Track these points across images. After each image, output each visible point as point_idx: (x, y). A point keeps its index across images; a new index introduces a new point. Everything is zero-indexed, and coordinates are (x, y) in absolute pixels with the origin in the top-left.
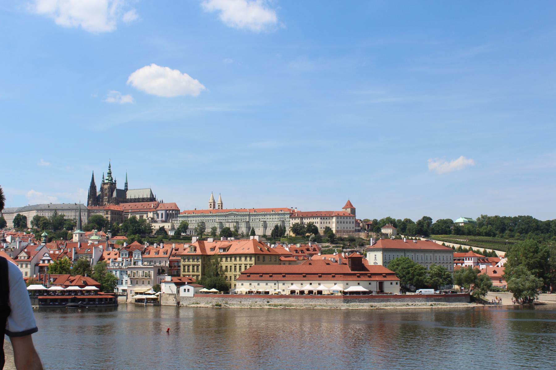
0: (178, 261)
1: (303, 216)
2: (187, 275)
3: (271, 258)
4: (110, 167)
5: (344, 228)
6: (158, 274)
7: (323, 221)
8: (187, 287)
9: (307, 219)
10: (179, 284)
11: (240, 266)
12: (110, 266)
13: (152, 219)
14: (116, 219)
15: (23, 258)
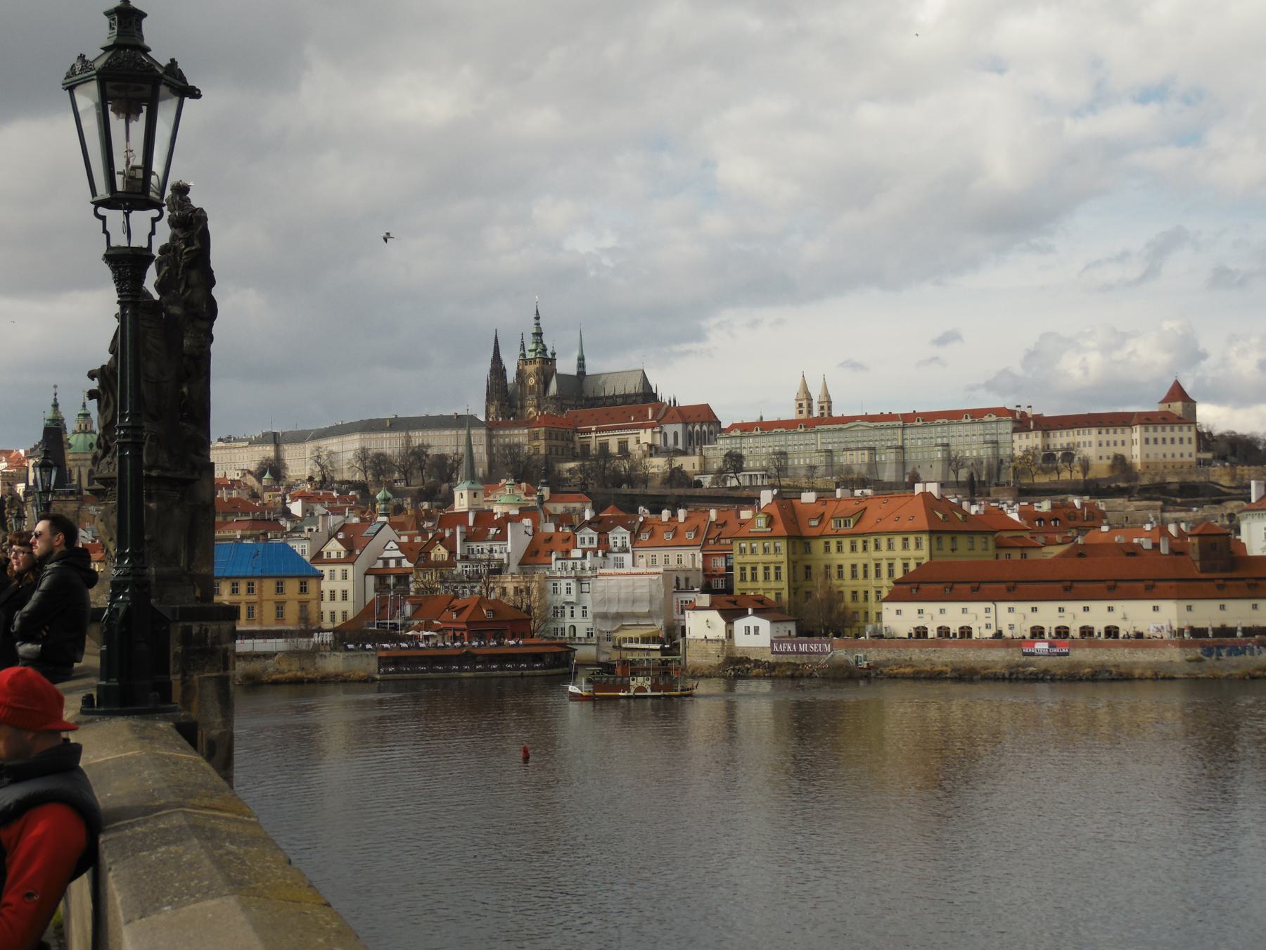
0: (727, 558)
1: (1047, 425)
2: (752, 589)
3: (972, 542)
4: (537, 318)
5: (1165, 456)
6: (675, 590)
7: (1105, 437)
8: (752, 621)
9: (1061, 436)
10: (732, 613)
11: (891, 565)
12: (553, 569)
13: (650, 446)
14: (560, 452)
15: (334, 555)
